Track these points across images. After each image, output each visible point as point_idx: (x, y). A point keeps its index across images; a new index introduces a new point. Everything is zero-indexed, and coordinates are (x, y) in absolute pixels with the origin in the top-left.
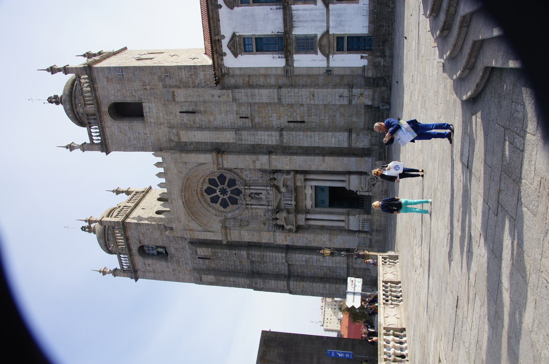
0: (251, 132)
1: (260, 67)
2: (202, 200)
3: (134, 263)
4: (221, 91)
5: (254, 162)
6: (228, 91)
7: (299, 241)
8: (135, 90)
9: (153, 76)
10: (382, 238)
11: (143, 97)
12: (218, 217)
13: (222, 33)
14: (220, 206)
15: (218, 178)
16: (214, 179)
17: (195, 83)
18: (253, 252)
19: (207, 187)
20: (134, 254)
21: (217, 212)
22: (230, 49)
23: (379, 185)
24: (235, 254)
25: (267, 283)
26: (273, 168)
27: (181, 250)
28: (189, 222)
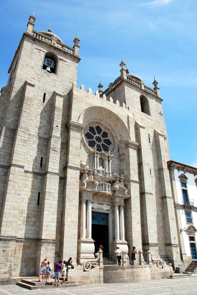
2: (94, 121)
5: (134, 170)
7: (71, 191)
10: (125, 279)
15: (108, 140)
16: (107, 137)
19: (102, 129)
20: (50, 49)
23: (158, 270)
24: (57, 126)
25: (23, 144)
26: (132, 183)
27: (53, 84)
28: (85, 103)
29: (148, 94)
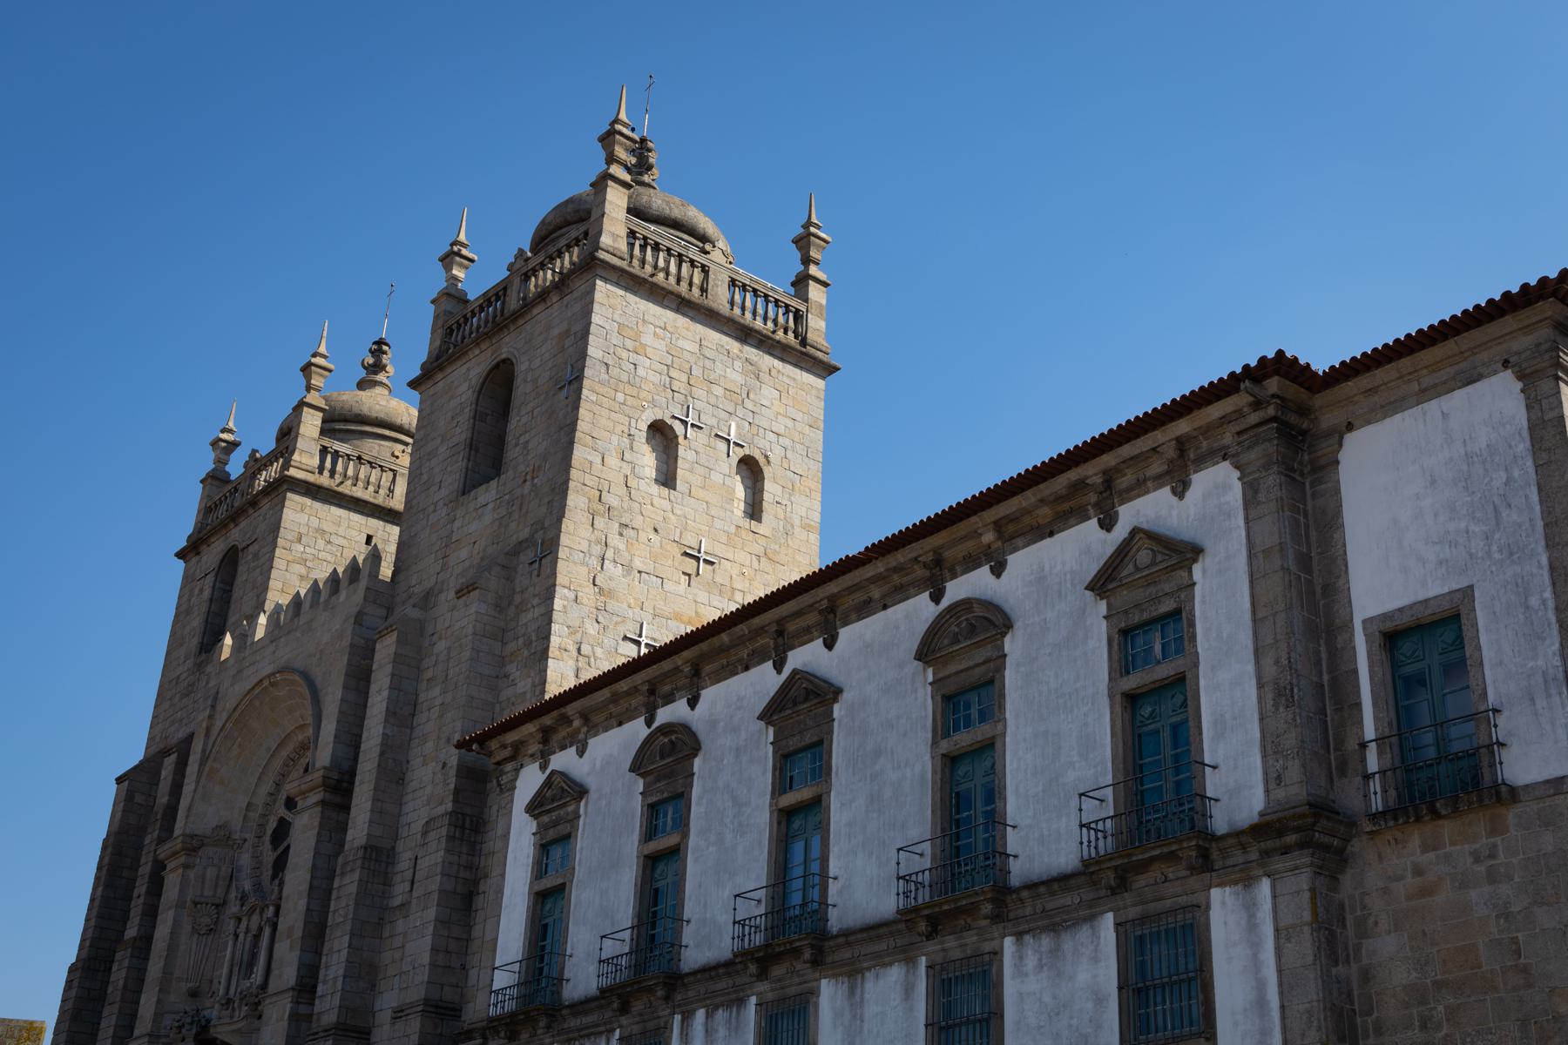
0: (351, 908)
1: (500, 916)
3: (213, 540)
4: (453, 772)
6: (451, 798)
8: (527, 442)
9: (546, 500)
11: (510, 474)
12: (241, 818)
13: (591, 742)
14: (279, 816)
17: (512, 662)
18: (126, 963)
21: (260, 810)
22: (548, 783)
29: (521, 322)
